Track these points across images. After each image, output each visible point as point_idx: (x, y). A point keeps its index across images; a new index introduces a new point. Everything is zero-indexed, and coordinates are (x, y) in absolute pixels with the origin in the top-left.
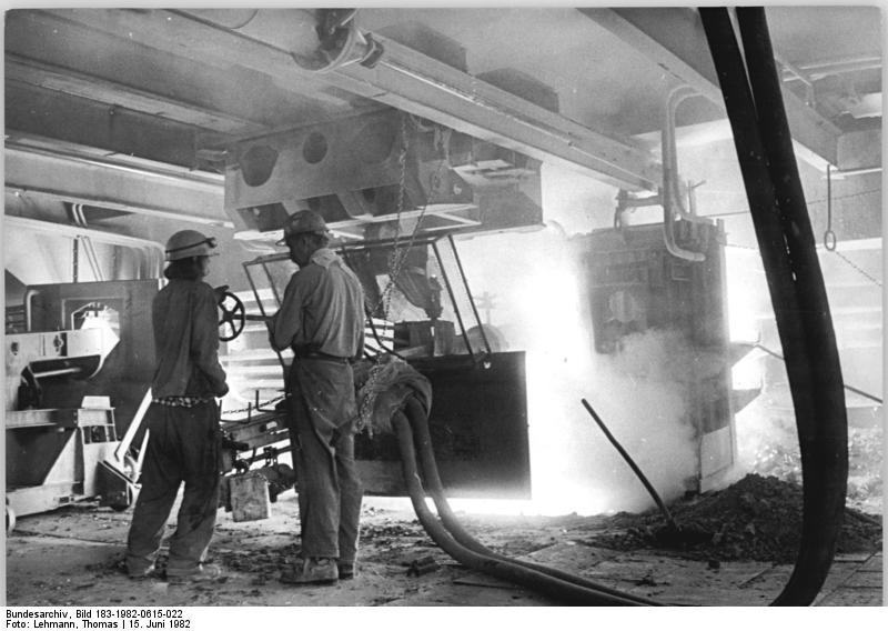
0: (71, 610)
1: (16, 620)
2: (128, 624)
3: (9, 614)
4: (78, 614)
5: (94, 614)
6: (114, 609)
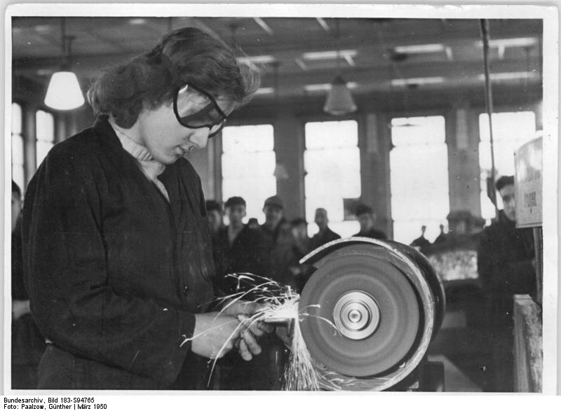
1: (10, 404)
3: (5, 400)
4: (50, 400)
5: (59, 400)
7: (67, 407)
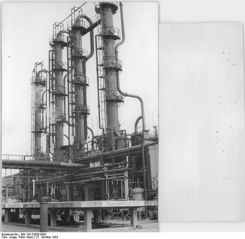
0: (20, 233)
1: (4, 236)
2: (36, 237)
3: (2, 234)
4: (22, 234)
5: (26, 234)
6: (31, 233)
7: (31, 237)
